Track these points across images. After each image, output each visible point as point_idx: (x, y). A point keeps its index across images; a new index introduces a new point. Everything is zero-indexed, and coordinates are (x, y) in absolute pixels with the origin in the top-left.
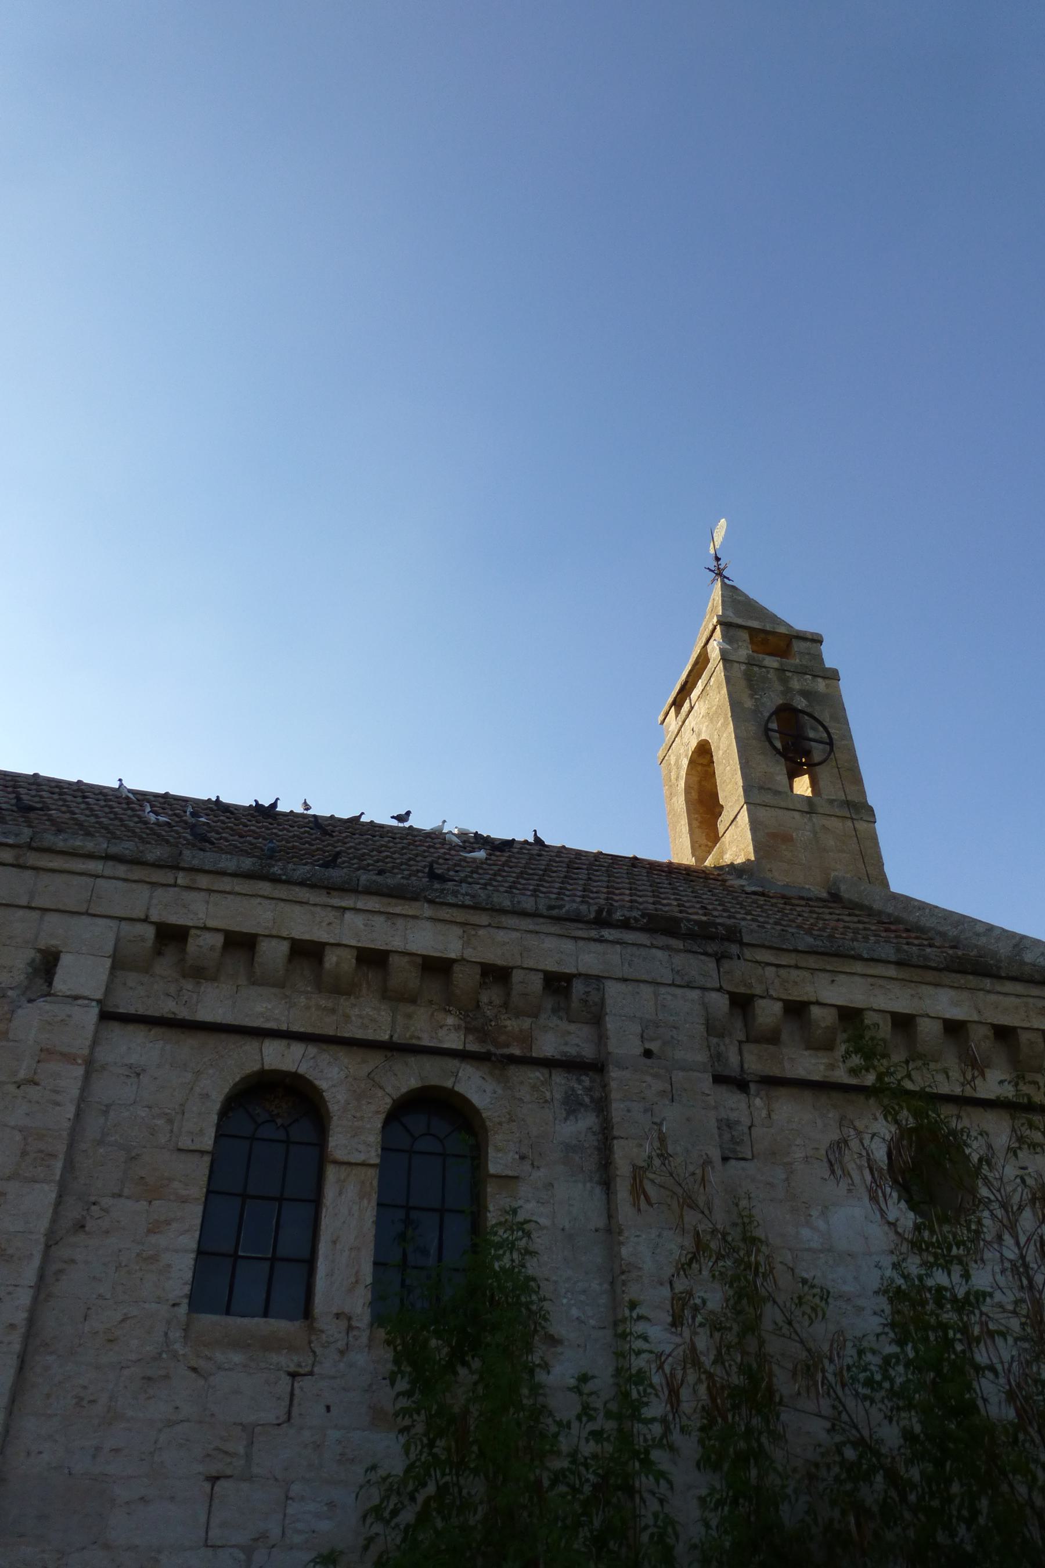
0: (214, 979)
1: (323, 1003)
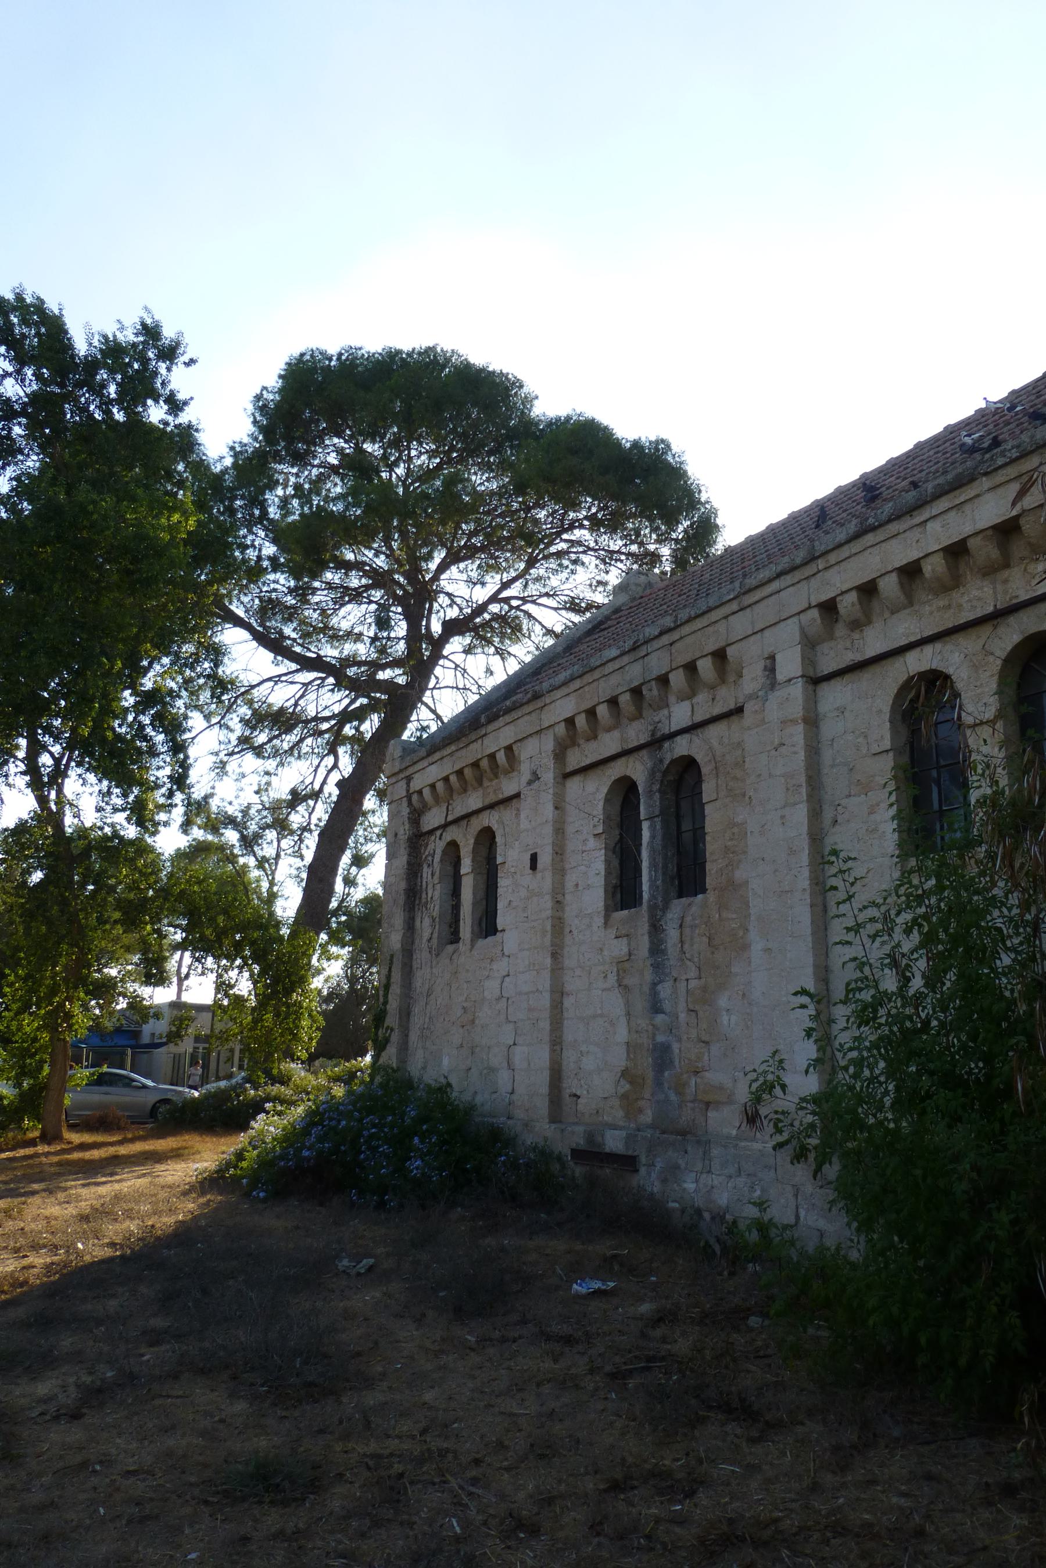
0: (869, 622)
1: (941, 603)
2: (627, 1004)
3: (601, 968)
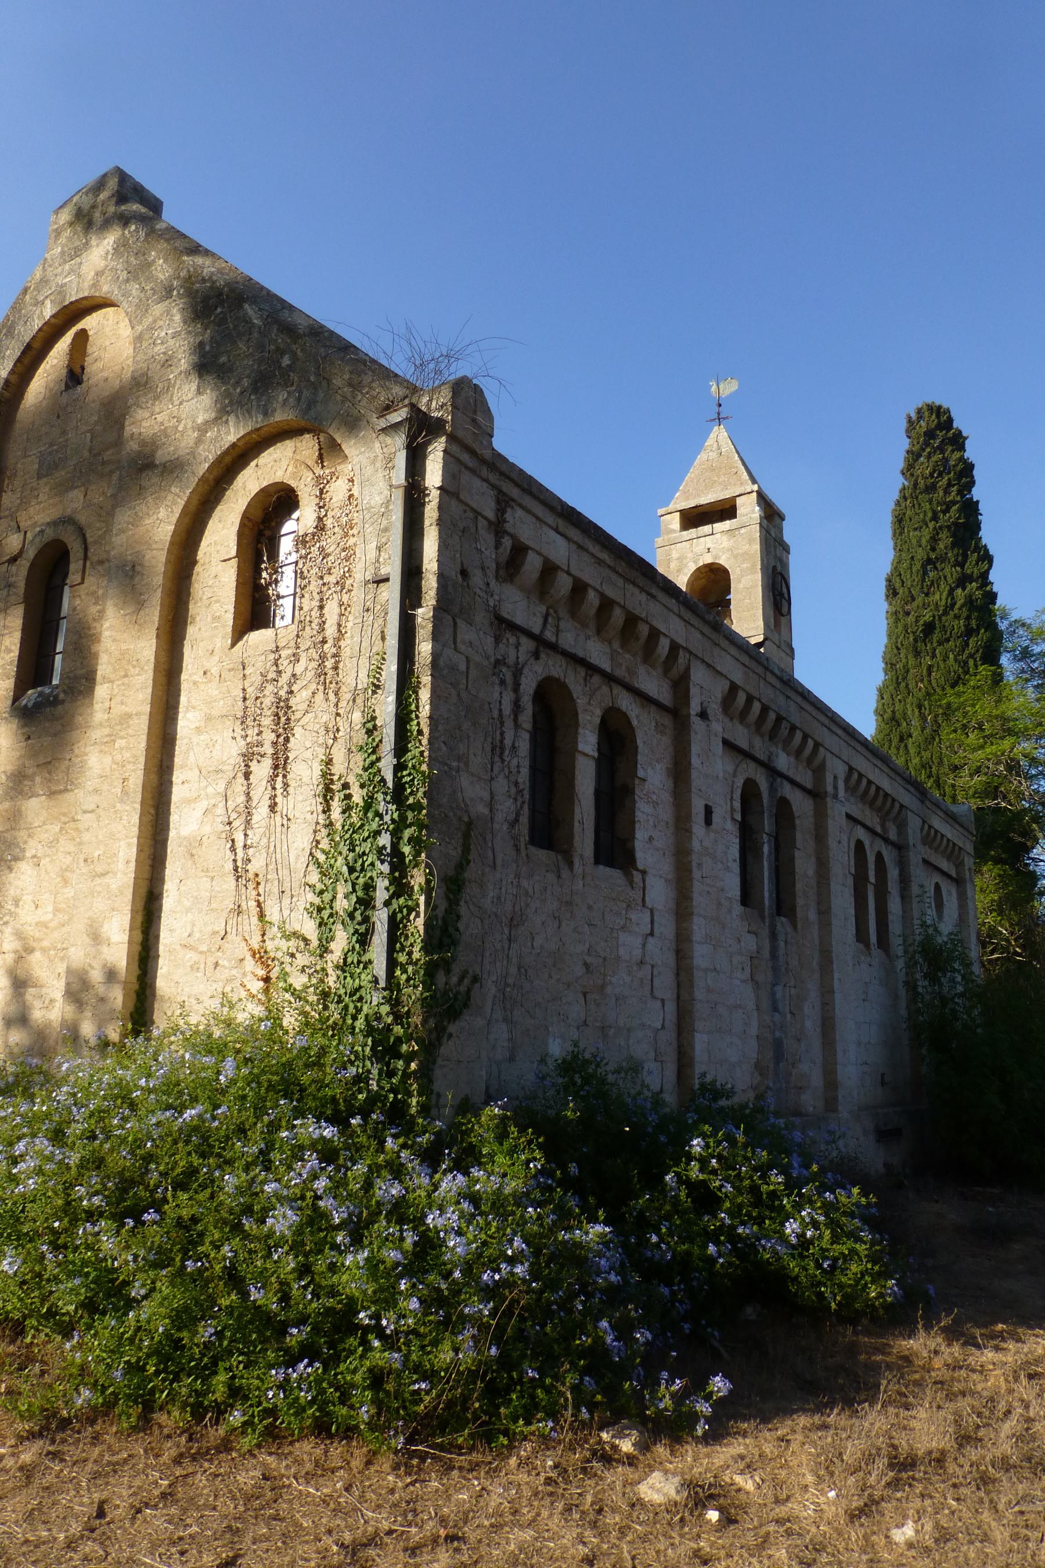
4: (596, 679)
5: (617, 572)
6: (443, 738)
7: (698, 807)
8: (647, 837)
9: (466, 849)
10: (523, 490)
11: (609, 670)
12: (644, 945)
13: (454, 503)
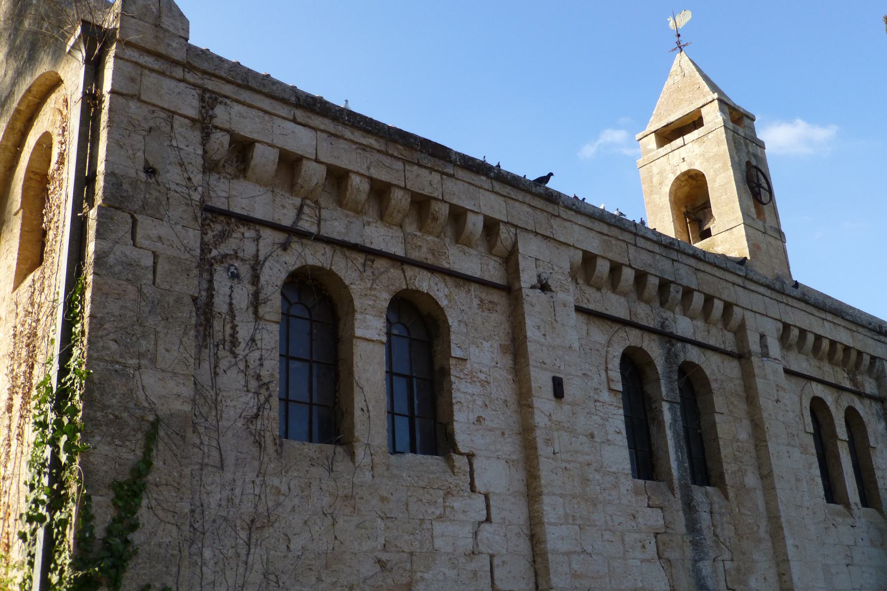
2: (671, 578)
3: (637, 536)
4: (380, 264)
5: (392, 156)
6: (112, 336)
7: (541, 381)
8: (473, 417)
9: (148, 450)
10: (239, 86)
11: (399, 251)
12: (476, 534)
13: (133, 105)
